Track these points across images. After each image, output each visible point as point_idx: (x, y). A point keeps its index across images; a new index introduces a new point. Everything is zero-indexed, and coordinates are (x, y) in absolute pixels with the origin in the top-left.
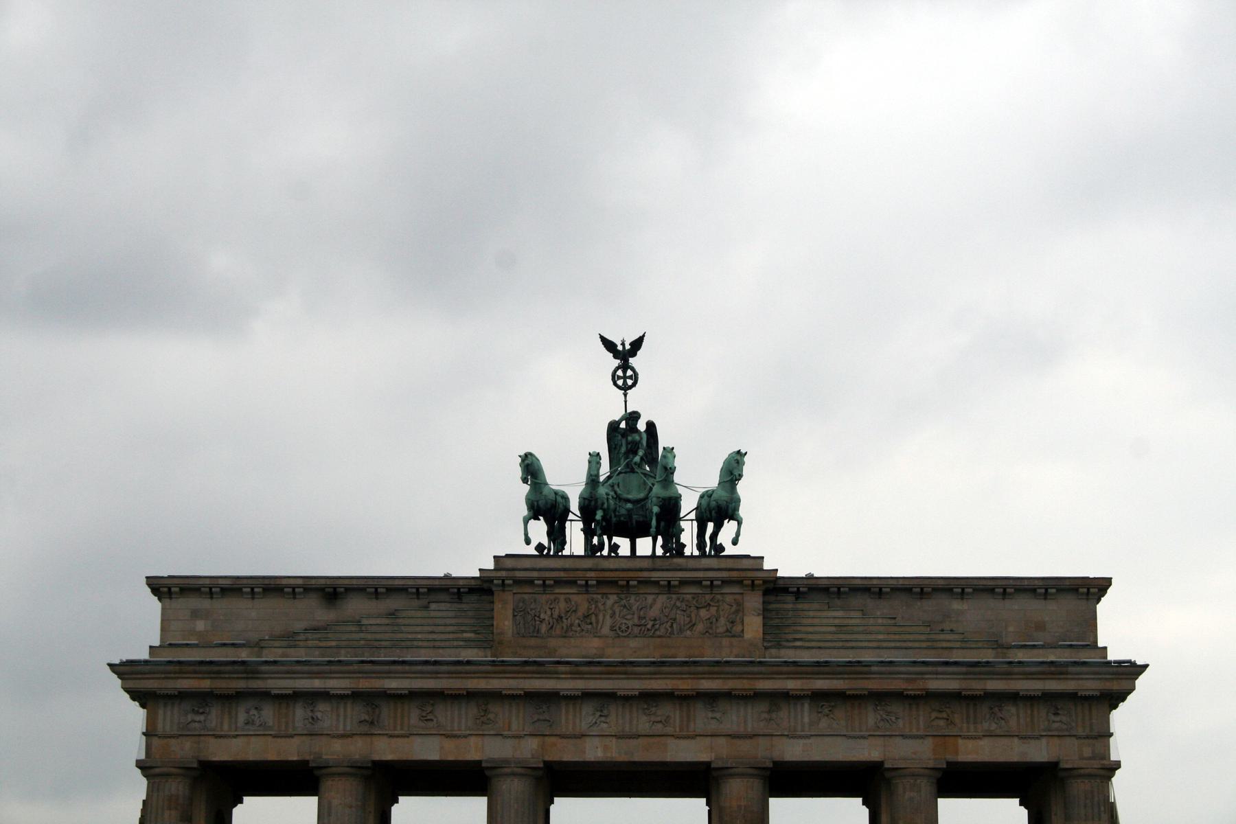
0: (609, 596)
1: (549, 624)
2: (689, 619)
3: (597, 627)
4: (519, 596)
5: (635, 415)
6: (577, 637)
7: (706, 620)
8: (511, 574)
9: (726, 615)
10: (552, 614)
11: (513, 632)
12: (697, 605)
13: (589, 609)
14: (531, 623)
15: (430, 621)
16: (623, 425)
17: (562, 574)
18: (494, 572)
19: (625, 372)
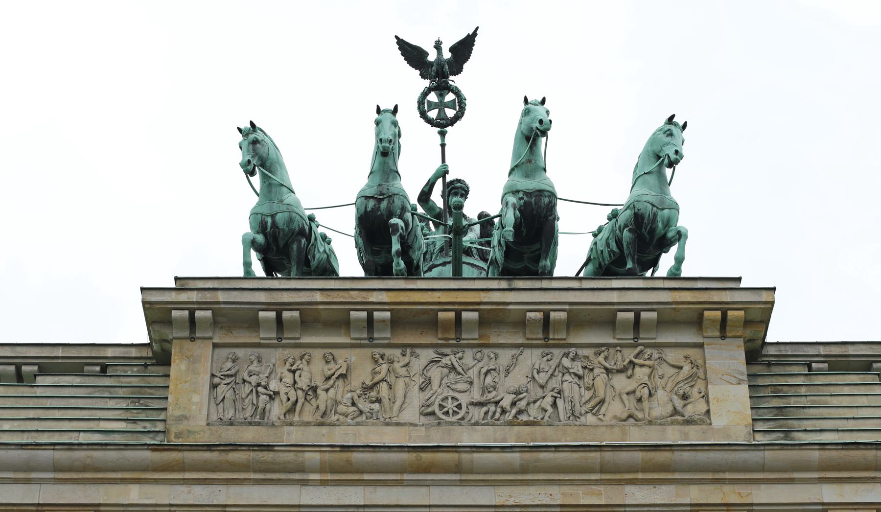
0: (418, 351)
1: (289, 399)
2: (588, 395)
3: (391, 408)
4: (225, 352)
5: (459, 184)
6: (348, 425)
7: (628, 394)
8: (208, 297)
9: (668, 389)
10: (295, 382)
11: (207, 420)
12: (607, 365)
13: (374, 373)
14: (247, 401)
15: (31, 403)
16: (437, 198)
17: (318, 297)
18: (174, 293)
19: (441, 96)
